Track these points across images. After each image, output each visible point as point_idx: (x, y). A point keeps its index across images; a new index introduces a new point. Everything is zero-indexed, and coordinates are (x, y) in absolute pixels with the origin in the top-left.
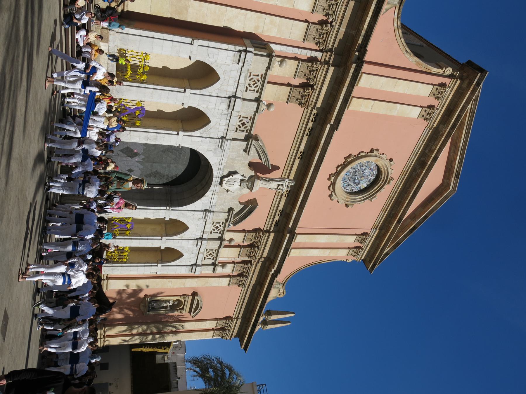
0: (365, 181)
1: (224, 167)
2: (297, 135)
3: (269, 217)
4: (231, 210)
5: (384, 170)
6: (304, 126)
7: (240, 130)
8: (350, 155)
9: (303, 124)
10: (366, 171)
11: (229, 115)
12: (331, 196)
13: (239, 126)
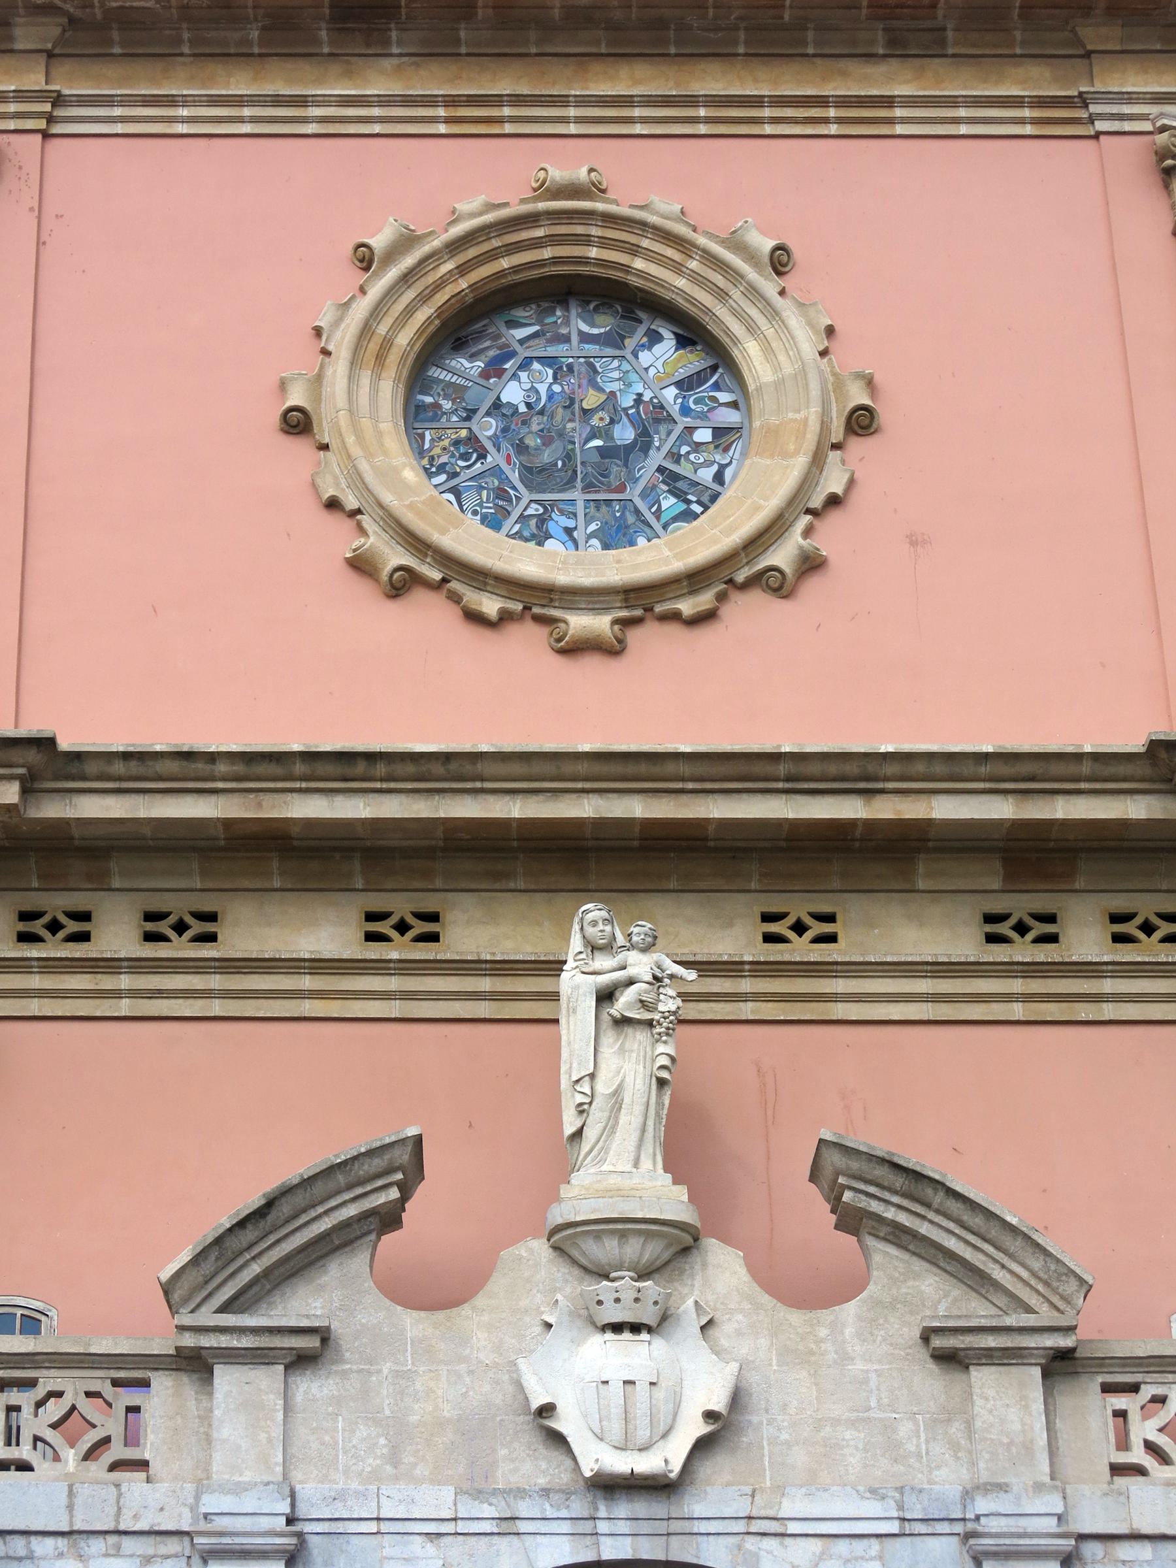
0: (611, 375)
1: (478, 1494)
2: (217, 1007)
3: (1084, 1011)
4: (950, 1354)
5: (463, 270)
6: (125, 982)
7: (132, 1438)
8: (361, 565)
9: (117, 994)
10: (513, 394)
12: (778, 585)
13: (89, 1455)
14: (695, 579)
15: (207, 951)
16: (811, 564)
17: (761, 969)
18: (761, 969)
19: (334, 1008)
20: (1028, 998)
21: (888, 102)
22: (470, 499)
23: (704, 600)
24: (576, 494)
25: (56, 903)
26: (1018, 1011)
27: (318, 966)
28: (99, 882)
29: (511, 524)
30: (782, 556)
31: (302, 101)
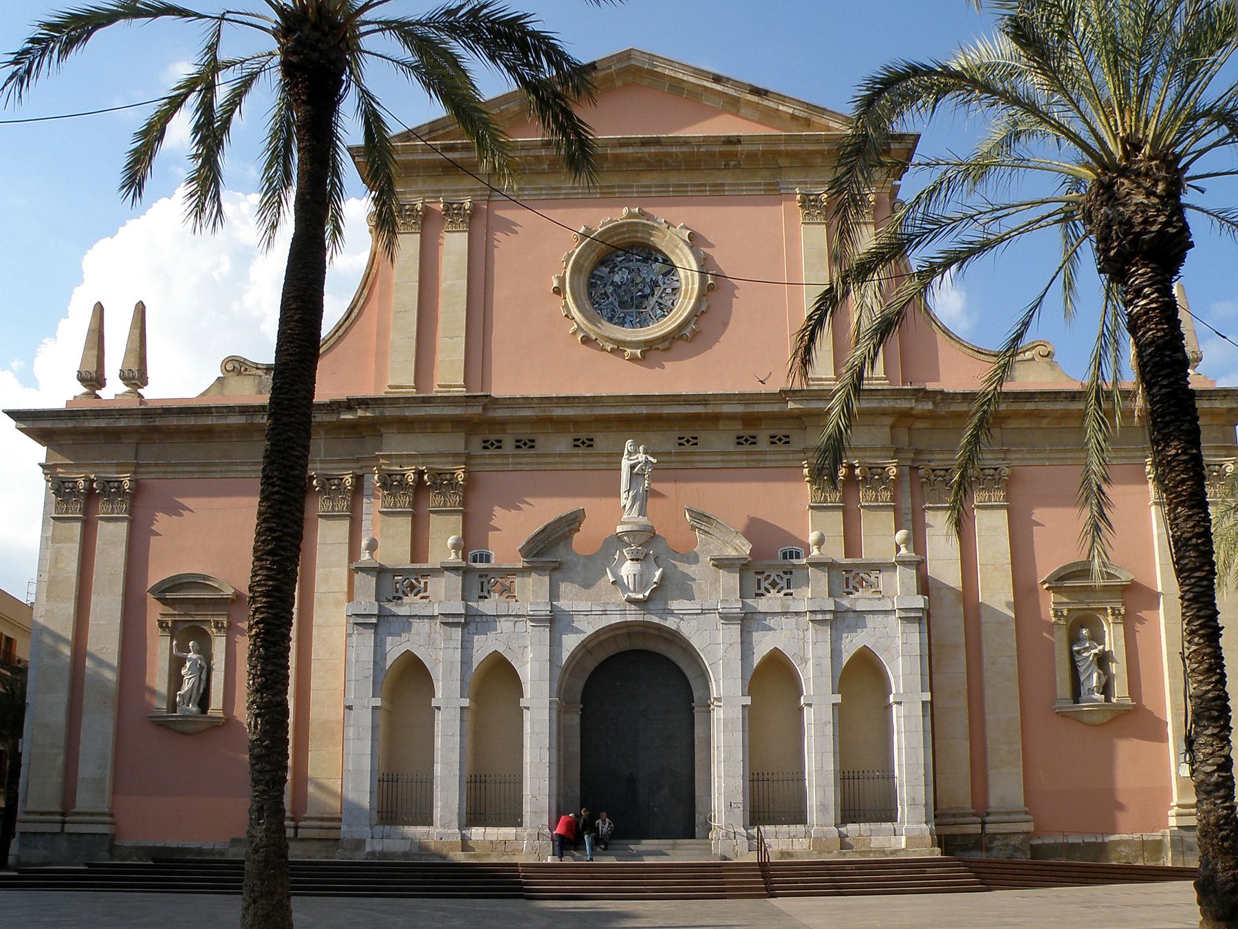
2: (535, 467)
10: (617, 278)
11: (478, 619)
14: (664, 338)
15: (533, 451)
16: (695, 333)
17: (678, 454)
18: (678, 454)
19: (565, 467)
20: (747, 461)
21: (723, 185)
22: (604, 312)
23: (667, 344)
24: (633, 310)
25: (493, 437)
26: (744, 464)
27: (561, 455)
28: (504, 432)
29: (616, 320)
30: (687, 332)
31: (558, 188)
